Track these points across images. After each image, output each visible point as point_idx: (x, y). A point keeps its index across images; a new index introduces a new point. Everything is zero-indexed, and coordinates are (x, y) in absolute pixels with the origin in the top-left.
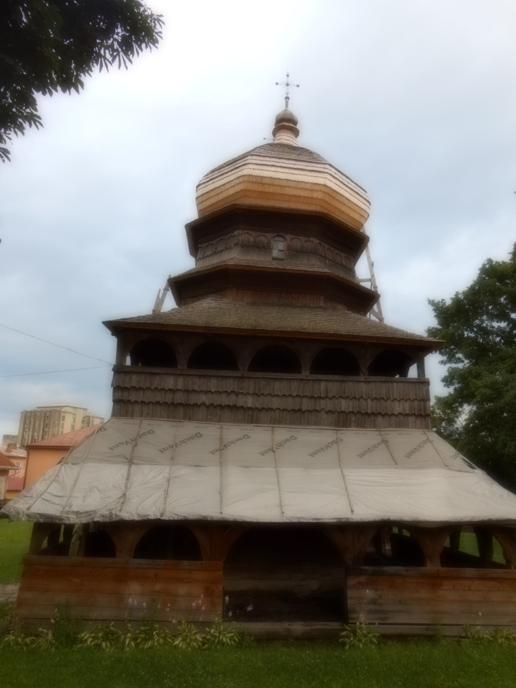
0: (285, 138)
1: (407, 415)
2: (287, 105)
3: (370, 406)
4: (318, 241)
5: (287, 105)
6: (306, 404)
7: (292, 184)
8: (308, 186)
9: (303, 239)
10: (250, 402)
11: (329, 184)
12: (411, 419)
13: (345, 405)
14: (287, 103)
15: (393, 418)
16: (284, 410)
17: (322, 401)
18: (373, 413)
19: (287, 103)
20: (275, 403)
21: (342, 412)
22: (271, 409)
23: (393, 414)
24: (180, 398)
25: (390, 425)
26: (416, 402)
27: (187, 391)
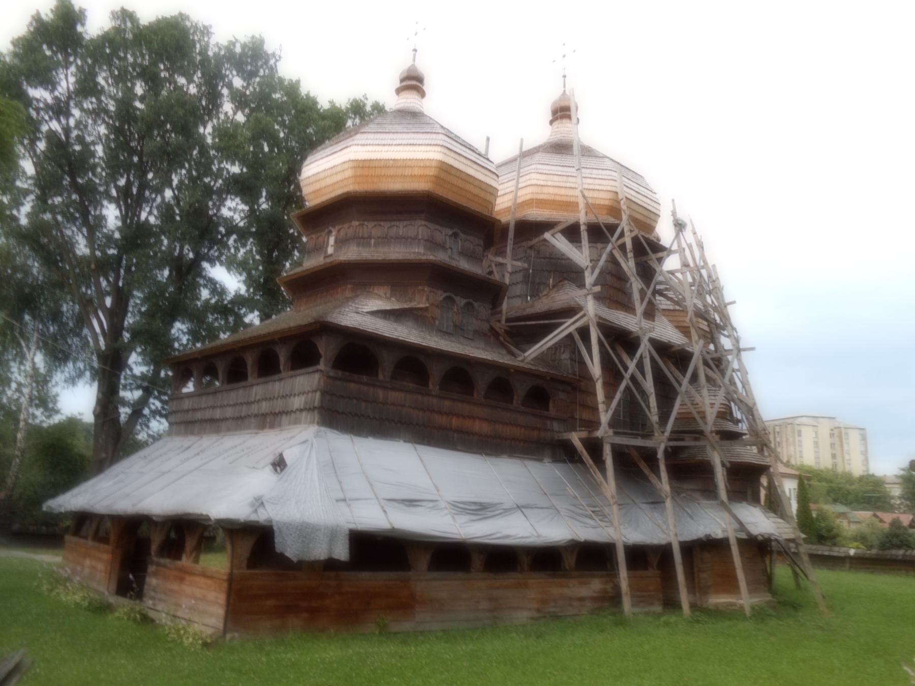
0: (409, 100)
1: (301, 410)
2: (414, 60)
3: (278, 405)
4: (357, 223)
5: (414, 60)
6: (244, 410)
7: (329, 172)
8: (339, 169)
9: (346, 226)
10: (218, 414)
11: (354, 156)
12: (304, 414)
13: (265, 407)
14: (415, 55)
15: (293, 415)
16: (233, 418)
17: (253, 406)
18: (280, 412)
19: (415, 55)
20: (229, 412)
21: (263, 414)
22: (226, 419)
23: (292, 411)
24: (189, 416)
25: (289, 424)
26: (310, 395)
27: (194, 410)
